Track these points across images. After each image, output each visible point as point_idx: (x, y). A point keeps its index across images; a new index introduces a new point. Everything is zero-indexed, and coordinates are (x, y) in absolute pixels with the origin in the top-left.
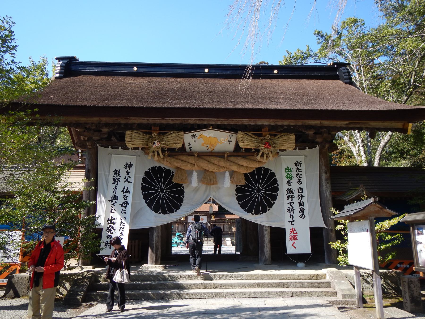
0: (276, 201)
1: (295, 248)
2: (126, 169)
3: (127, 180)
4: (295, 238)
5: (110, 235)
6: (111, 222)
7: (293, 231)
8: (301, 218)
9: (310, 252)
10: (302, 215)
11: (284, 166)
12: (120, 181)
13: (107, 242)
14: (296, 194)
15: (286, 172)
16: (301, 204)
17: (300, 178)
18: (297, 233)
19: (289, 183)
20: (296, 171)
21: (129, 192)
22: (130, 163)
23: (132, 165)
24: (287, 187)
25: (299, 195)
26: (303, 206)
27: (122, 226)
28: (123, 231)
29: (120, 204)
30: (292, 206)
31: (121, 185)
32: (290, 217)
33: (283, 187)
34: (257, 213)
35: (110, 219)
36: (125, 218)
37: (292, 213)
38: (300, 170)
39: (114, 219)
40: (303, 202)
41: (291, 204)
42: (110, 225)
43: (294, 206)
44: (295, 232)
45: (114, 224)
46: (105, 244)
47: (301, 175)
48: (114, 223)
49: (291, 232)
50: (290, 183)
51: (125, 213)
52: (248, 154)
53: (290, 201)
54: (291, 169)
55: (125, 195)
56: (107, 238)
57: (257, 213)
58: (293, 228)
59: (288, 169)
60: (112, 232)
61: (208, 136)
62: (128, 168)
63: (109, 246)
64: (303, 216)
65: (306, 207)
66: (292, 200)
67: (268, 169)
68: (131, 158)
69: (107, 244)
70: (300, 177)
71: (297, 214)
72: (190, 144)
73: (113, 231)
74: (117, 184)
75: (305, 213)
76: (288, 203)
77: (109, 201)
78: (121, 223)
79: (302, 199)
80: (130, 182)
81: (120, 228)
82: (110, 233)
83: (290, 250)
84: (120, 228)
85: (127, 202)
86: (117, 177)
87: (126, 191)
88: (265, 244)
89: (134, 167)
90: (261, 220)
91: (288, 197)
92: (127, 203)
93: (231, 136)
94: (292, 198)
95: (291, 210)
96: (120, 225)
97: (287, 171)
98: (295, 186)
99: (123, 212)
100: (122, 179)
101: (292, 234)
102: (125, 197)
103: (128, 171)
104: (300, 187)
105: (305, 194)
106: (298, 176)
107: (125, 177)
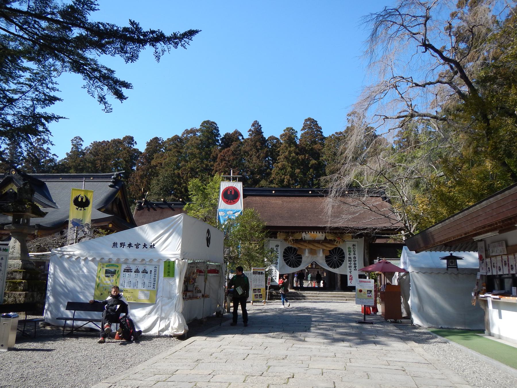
4: (351, 279)
7: (351, 276)
11: (348, 246)
14: (353, 259)
16: (355, 264)
19: (349, 254)
24: (348, 256)
33: (347, 256)
52: (331, 242)
57: (335, 268)
68: (278, 243)
71: (353, 268)
90: (336, 271)
91: (349, 261)
98: (352, 256)
105: (357, 259)
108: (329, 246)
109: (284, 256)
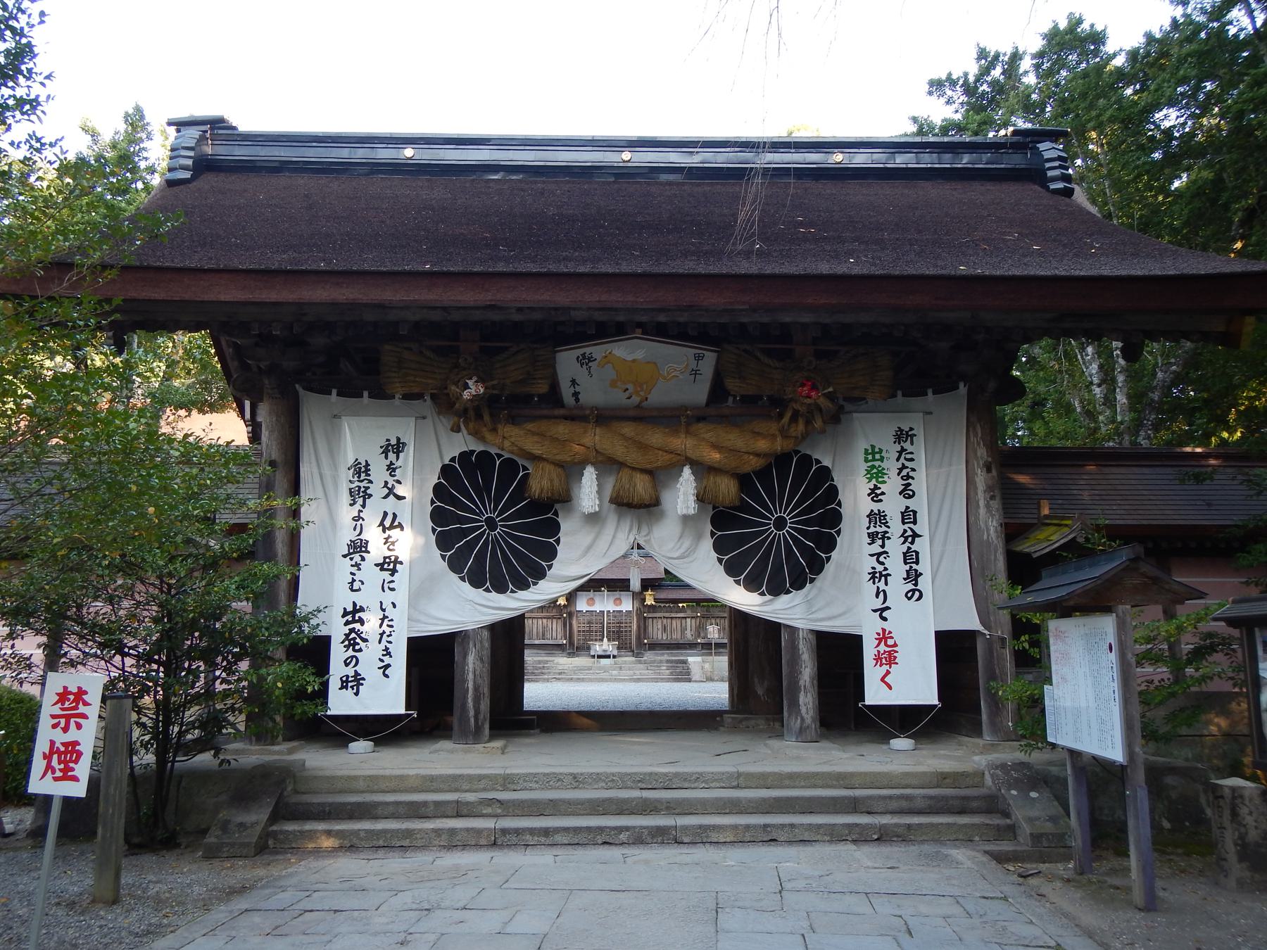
0: (834, 554)
1: (890, 687)
2: (386, 458)
4: (889, 659)
5: (352, 657)
6: (354, 617)
7: (883, 637)
8: (909, 599)
9: (936, 702)
10: (913, 591)
12: (370, 496)
13: (347, 676)
14: (896, 527)
15: (866, 460)
16: (911, 557)
17: (910, 481)
18: (895, 645)
20: (898, 460)
21: (401, 526)
22: (398, 439)
23: (404, 444)
24: (867, 505)
25: (905, 531)
26: (917, 563)
27: (384, 627)
28: (390, 642)
30: (882, 563)
32: (877, 596)
34: (776, 589)
35: (350, 608)
36: (394, 606)
37: (882, 585)
38: (909, 456)
39: (362, 609)
40: (917, 553)
41: (881, 559)
43: (888, 563)
44: (890, 642)
45: (362, 624)
46: (343, 682)
47: (913, 470)
48: (361, 621)
49: (880, 640)
50: (877, 495)
51: (392, 590)
53: (876, 548)
54: (881, 451)
56: (347, 665)
58: (884, 630)
59: (873, 453)
61: (629, 358)
62: (392, 456)
63: (352, 687)
64: (917, 594)
65: (924, 566)
66: (883, 546)
67: (810, 457)
68: (402, 427)
69: (347, 681)
70: (908, 477)
71: (897, 586)
72: (574, 382)
73: (362, 645)
74: (364, 506)
75: (925, 583)
76: (872, 555)
77: (345, 556)
78: (383, 620)
79: (912, 543)
80: (400, 498)
81: (382, 635)
82: (354, 650)
83: (875, 694)
84: (382, 635)
85: (397, 558)
86: (362, 485)
88: (802, 683)
89: (410, 450)
91: (873, 537)
93: (698, 358)
94: (883, 538)
95: (881, 575)
96: (381, 626)
97: (870, 457)
98: (893, 505)
99: (386, 586)
100: (377, 490)
101: (882, 648)
103: (392, 463)
104: (907, 508)
105: (922, 527)
106: (904, 472)
107: (386, 483)
108: (735, 439)
109: (438, 516)
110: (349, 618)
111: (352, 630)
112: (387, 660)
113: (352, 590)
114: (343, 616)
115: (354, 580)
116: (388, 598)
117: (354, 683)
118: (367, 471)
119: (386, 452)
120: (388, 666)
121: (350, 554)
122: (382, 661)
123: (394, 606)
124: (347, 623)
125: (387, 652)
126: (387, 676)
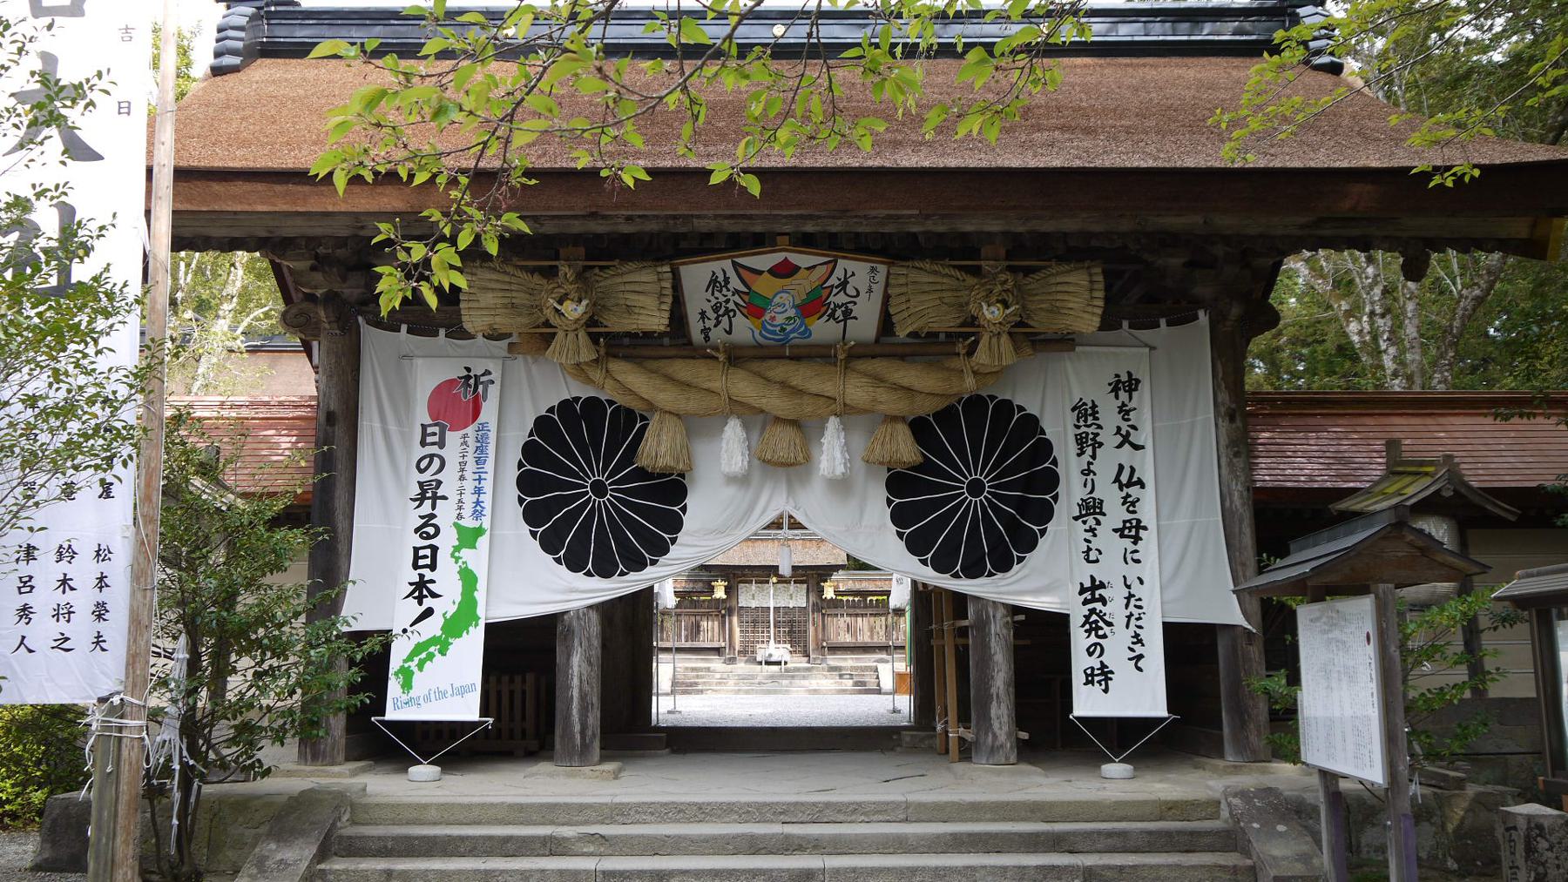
2: (1117, 397)
3: (1126, 439)
5: (1095, 644)
6: (1093, 594)
12: (1101, 444)
22: (1130, 374)
23: (1138, 381)
29: (1115, 530)
31: (1109, 459)
35: (1087, 584)
36: (1141, 582)
39: (1102, 586)
42: (1090, 606)
45: (1105, 604)
48: (1103, 601)
51: (1138, 561)
55: (1128, 496)
56: (1090, 654)
60: (1101, 633)
62: (1123, 396)
69: (1092, 675)
73: (1107, 629)
74: (1094, 457)
77: (1076, 518)
80: (1137, 447)
81: (1129, 617)
82: (1097, 636)
85: (1139, 521)
86: (1089, 430)
87: (1128, 481)
89: (1145, 387)
92: (1139, 526)
96: (1127, 606)
100: (1108, 438)
102: (1130, 503)
103: (1124, 404)
107: (1119, 429)
110: (1088, 595)
111: (1092, 611)
112: (1139, 649)
113: (1088, 561)
114: (1081, 593)
115: (1089, 549)
116: (1133, 571)
117: (1102, 676)
118: (1094, 414)
119: (1115, 390)
120: (1140, 657)
121: (1081, 516)
122: (1132, 650)
123: (1141, 582)
124: (1085, 602)
125: (1138, 640)
126: (1140, 669)
